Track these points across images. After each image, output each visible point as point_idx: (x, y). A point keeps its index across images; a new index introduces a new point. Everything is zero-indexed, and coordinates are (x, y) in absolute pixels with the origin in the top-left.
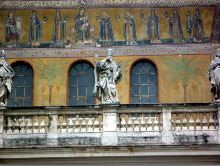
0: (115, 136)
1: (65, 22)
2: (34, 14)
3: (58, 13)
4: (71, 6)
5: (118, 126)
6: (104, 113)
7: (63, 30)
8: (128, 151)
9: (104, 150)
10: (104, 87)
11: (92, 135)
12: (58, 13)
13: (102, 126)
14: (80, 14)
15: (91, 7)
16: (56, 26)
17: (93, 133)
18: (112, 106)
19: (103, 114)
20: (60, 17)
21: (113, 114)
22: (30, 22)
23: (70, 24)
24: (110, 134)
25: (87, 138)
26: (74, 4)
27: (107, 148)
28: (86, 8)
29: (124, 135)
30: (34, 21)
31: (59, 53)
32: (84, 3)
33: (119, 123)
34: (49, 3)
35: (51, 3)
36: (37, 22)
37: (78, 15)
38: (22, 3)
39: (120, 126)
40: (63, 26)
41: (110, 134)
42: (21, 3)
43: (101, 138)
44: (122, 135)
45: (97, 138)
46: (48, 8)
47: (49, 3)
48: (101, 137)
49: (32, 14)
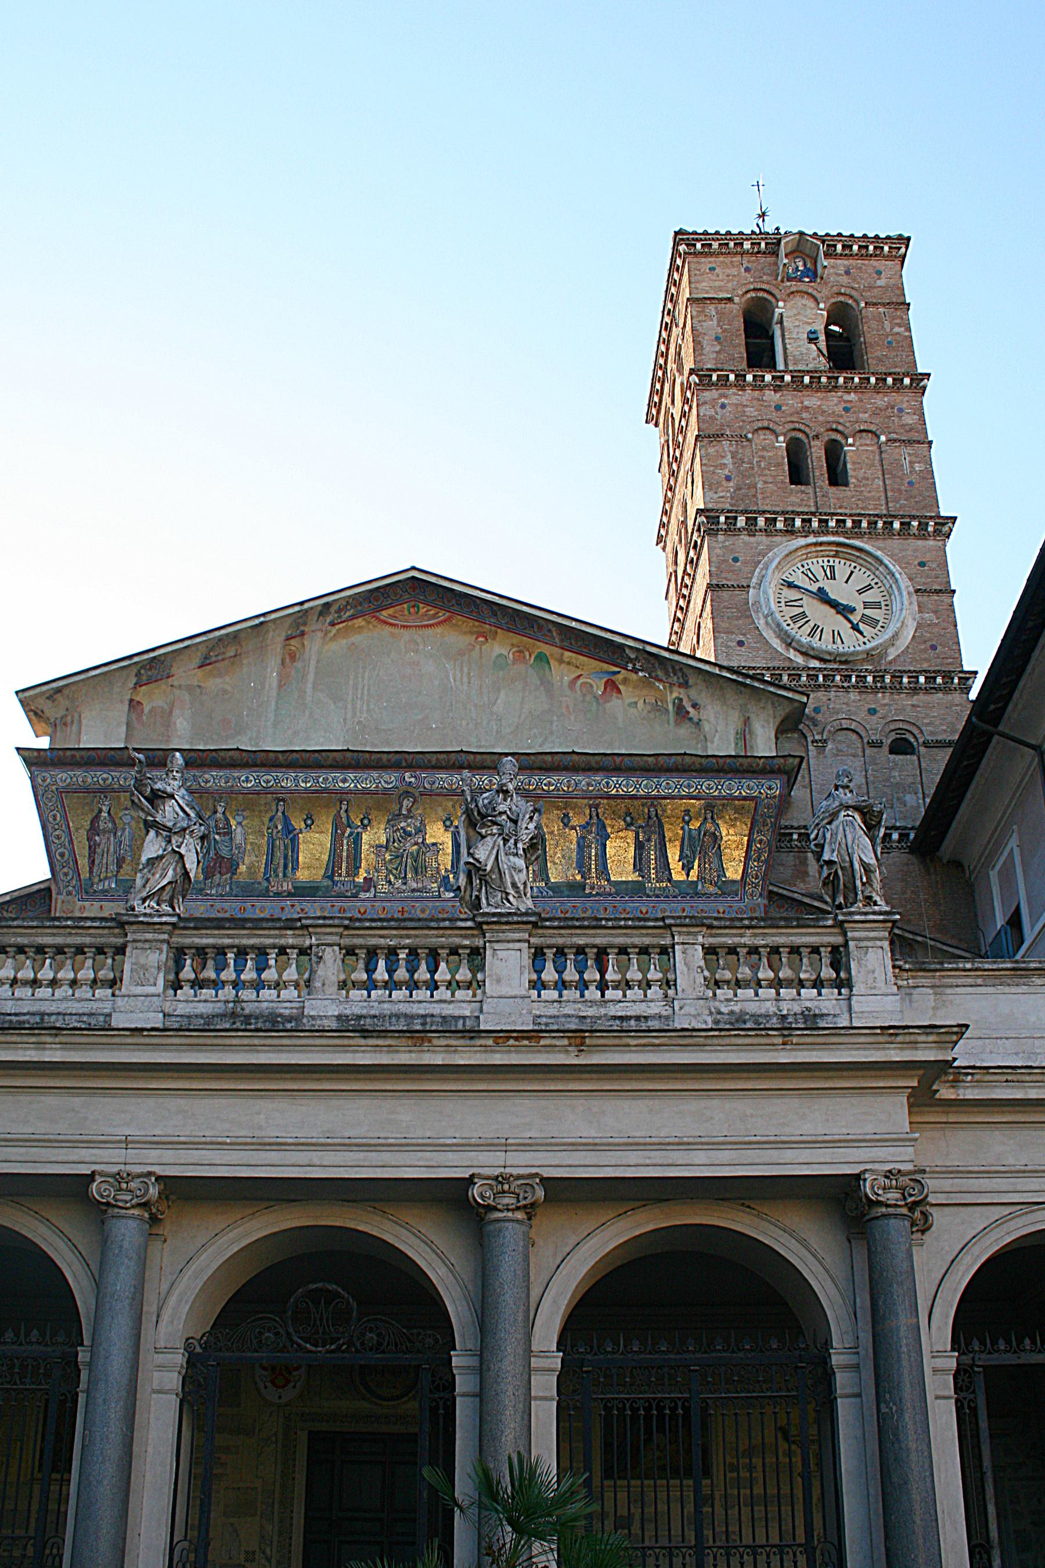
0: (524, 1012)
1: (359, 830)
2: (281, 809)
3: (344, 807)
4: (377, 787)
5: (533, 985)
6: (489, 941)
7: (356, 849)
8: (570, 1049)
9: (490, 1042)
10: (488, 868)
11: (449, 1010)
12: (344, 807)
13: (481, 985)
14: (400, 809)
15: (431, 791)
16: (336, 840)
17: (452, 1002)
18: (515, 918)
19: (485, 948)
20: (348, 817)
21: (518, 945)
22: (268, 828)
23: (374, 836)
24: (505, 1005)
25: (432, 1016)
26: (386, 782)
27: (503, 1037)
28: (417, 794)
29: (553, 1010)
30: (280, 827)
31: (342, 910)
32: (413, 780)
33: (534, 977)
34: (321, 780)
35: (326, 780)
36: (289, 829)
37: (397, 812)
38: (251, 778)
39: (538, 985)
40: (357, 840)
41: (505, 1005)
42: (247, 778)
43: (478, 1017)
44: (545, 1009)
45: (464, 1018)
46: (316, 792)
47: (321, 780)
48: (476, 1014)
49: (274, 807)
